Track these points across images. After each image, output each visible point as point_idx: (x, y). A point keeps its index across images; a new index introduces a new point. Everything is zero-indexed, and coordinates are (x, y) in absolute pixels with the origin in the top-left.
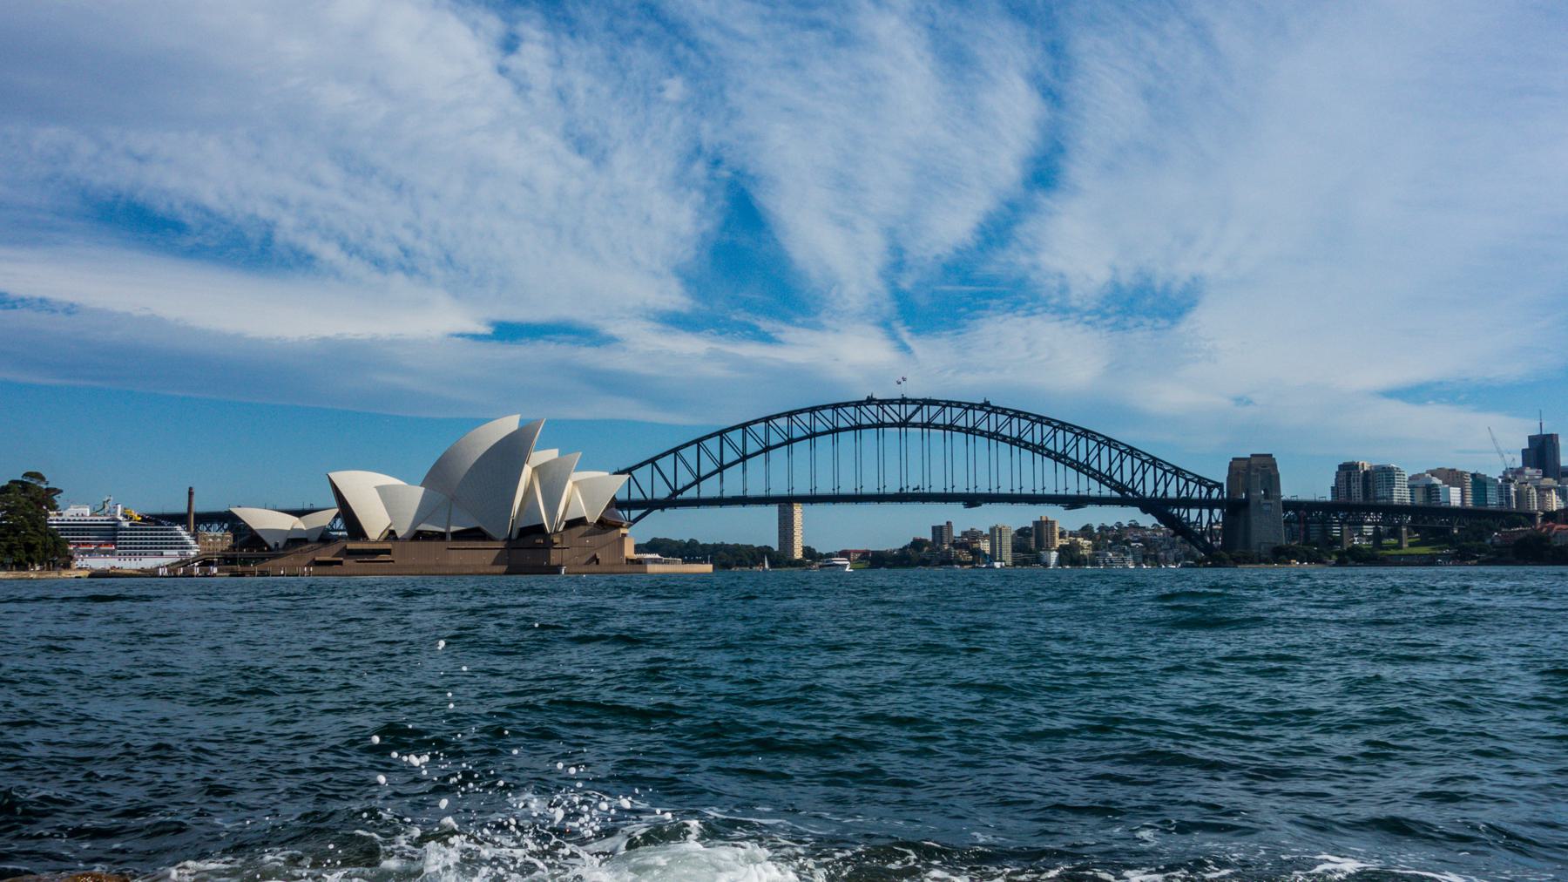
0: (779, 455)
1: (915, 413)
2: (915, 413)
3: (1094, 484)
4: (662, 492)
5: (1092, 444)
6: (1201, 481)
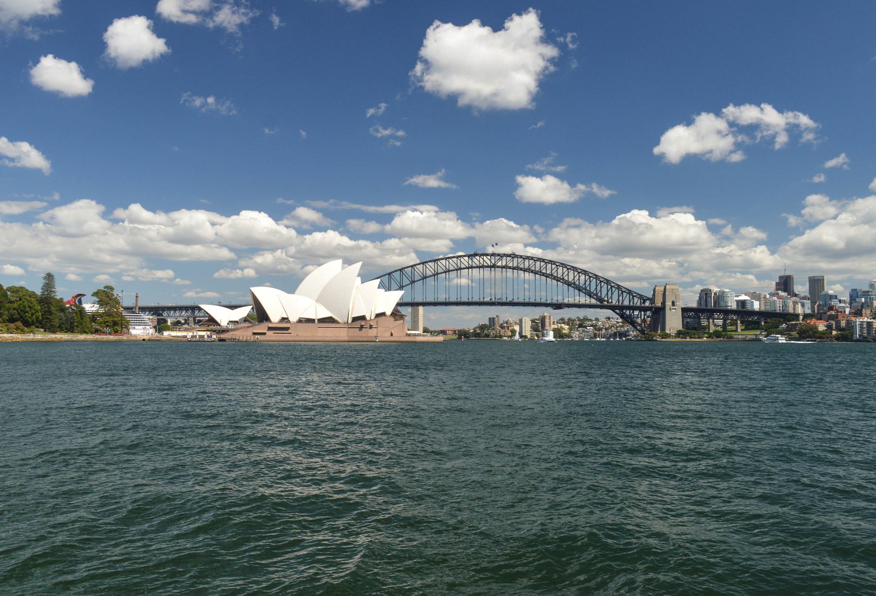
0: (430, 282)
5: (587, 277)
6: (641, 297)
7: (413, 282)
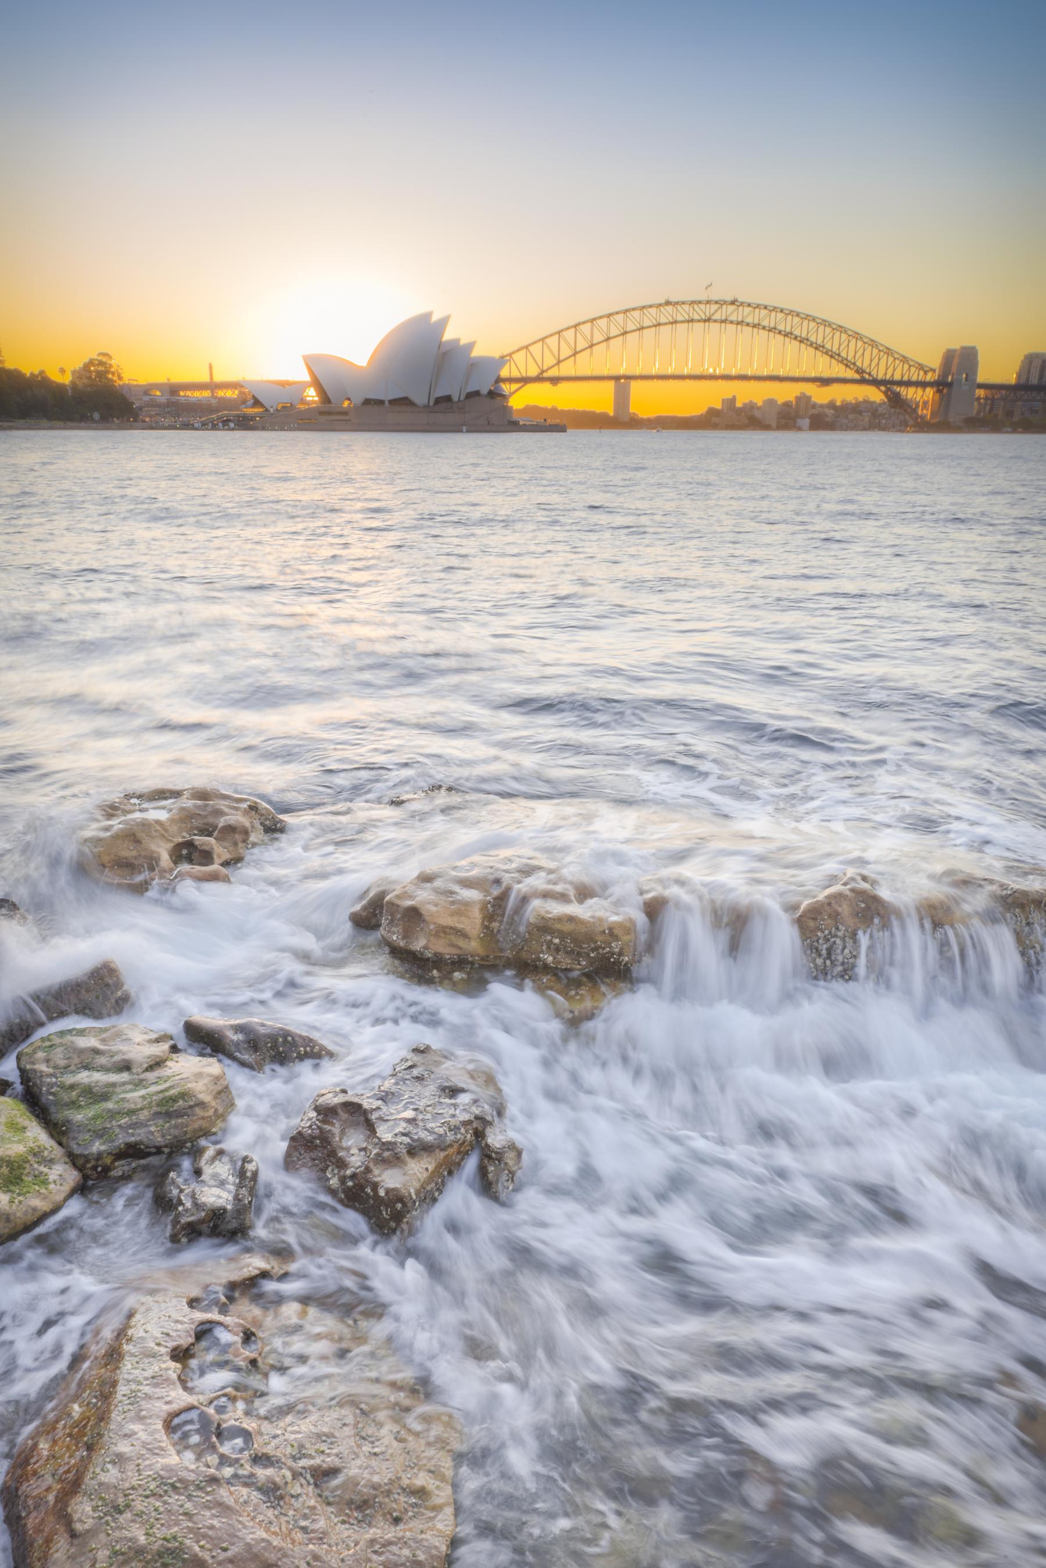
1: (716, 311)
2: (716, 311)
3: (842, 367)
4: (533, 372)
6: (921, 367)
7: (591, 346)
